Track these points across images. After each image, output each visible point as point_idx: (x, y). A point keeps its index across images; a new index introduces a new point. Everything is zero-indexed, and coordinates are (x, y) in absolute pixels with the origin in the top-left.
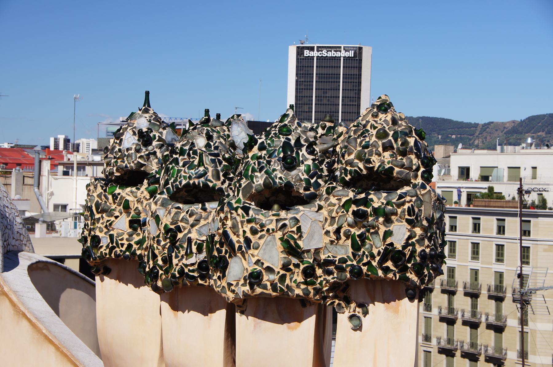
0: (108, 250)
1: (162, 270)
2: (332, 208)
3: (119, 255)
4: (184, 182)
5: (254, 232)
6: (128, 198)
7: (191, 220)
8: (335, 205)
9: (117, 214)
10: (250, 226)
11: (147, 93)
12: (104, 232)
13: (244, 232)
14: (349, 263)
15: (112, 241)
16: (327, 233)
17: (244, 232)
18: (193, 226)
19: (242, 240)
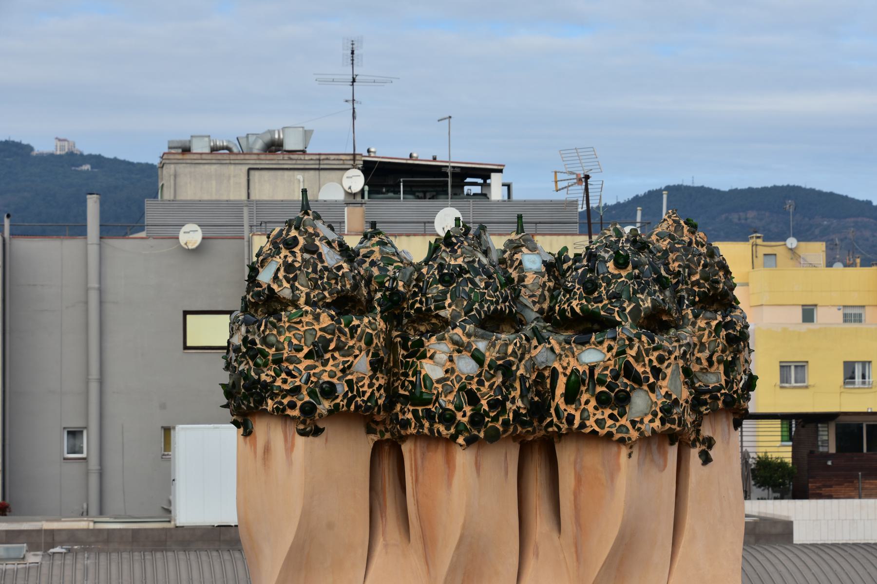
0: (345, 401)
1: (489, 417)
3: (361, 406)
4: (492, 308)
5: (661, 359)
6: (368, 330)
7: (519, 353)
8: (704, 329)
9: (357, 352)
10: (656, 354)
13: (651, 361)
14: (723, 391)
15: (351, 388)
16: (698, 359)
17: (651, 361)
18: (520, 361)
19: (648, 370)
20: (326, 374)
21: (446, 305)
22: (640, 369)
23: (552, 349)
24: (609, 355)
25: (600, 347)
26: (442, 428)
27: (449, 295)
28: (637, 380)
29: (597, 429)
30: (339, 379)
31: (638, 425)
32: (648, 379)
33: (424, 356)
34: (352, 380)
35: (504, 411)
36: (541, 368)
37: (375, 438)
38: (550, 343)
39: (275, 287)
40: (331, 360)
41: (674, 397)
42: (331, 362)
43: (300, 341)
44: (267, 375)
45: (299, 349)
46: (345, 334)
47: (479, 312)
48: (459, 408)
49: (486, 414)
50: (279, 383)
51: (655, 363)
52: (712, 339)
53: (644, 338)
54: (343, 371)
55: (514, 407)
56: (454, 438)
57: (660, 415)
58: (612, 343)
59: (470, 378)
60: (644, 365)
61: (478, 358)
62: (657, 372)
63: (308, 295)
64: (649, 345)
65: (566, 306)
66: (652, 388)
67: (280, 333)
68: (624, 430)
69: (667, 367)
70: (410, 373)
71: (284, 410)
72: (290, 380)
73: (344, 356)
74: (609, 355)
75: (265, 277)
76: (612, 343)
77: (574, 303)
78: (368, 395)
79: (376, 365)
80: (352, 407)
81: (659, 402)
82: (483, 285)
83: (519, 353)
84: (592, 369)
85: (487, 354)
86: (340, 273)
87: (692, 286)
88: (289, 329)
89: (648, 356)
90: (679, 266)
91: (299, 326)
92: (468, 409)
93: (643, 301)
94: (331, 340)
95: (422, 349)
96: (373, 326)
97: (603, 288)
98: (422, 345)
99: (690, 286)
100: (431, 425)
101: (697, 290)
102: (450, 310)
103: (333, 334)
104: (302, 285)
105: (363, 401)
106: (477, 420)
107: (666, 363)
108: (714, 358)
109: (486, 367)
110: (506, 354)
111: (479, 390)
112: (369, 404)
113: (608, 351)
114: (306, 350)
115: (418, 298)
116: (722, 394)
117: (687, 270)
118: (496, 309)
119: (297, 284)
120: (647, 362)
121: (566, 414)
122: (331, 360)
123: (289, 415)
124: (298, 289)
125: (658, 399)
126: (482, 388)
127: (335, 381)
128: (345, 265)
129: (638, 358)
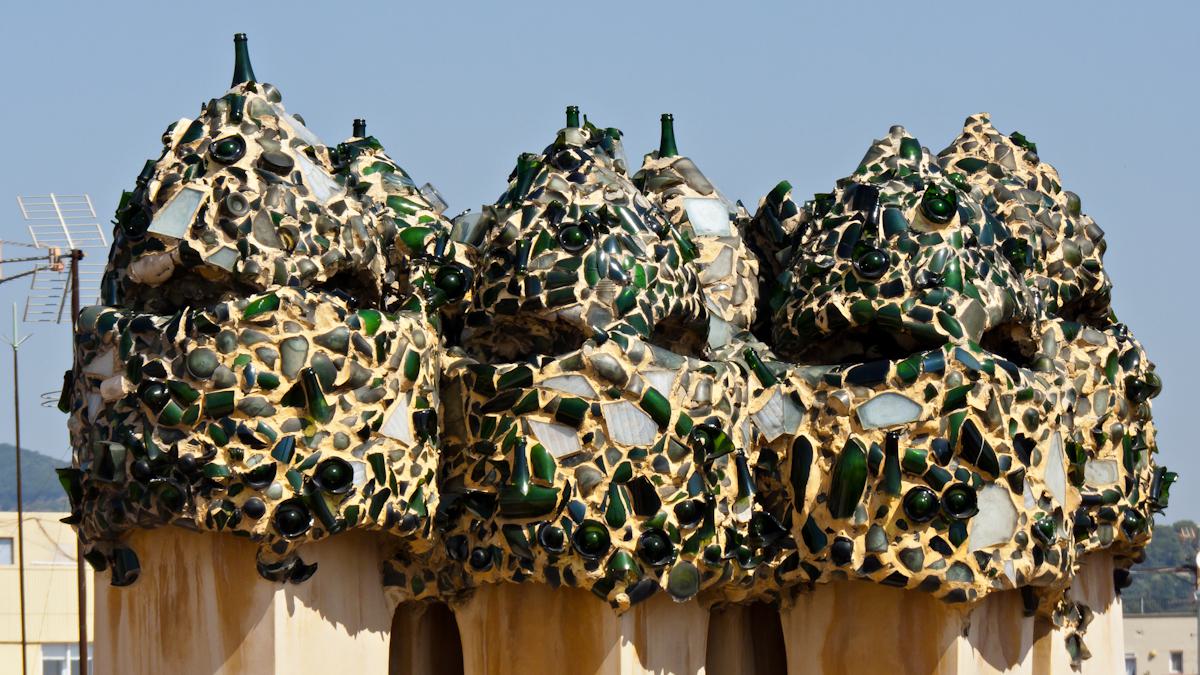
0: (369, 502)
2: (1080, 372)
4: (672, 302)
5: (1032, 421)
7: (732, 401)
9: (390, 395)
11: (240, 42)
12: (350, 449)
13: (1013, 423)
15: (380, 473)
17: (1013, 423)
19: (1009, 443)
20: (328, 440)
21: (577, 293)
22: (990, 439)
23: (795, 397)
24: (928, 408)
25: (908, 392)
26: (577, 566)
27: (581, 271)
28: (988, 466)
29: (904, 572)
30: (355, 452)
31: (992, 564)
32: (1008, 463)
33: (532, 405)
34: (380, 456)
35: (710, 528)
36: (770, 439)
37: (397, 594)
38: (788, 383)
39: (197, 245)
40: (339, 410)
41: (1055, 504)
42: (339, 414)
43: (271, 366)
44: (194, 442)
45: (268, 384)
46: (367, 353)
47: (647, 309)
48: (617, 521)
49: (677, 534)
50: (220, 460)
51: (1021, 429)
52: (1100, 386)
53: (1000, 373)
54: (364, 434)
55: (728, 523)
56: (604, 587)
57: (1031, 544)
58: (936, 383)
59: (636, 454)
60: (1000, 434)
61: (655, 409)
62: (1025, 447)
63: (279, 264)
64: (1010, 387)
65: (814, 305)
66: (1017, 483)
67: (222, 347)
68: (962, 573)
69: (1044, 437)
70: (499, 445)
71: (236, 520)
72: (248, 452)
73: (365, 401)
74: (928, 408)
75: (170, 223)
76: (936, 383)
77: (837, 299)
78: (410, 490)
79: (424, 425)
80: (382, 517)
81: (1031, 515)
82: (650, 251)
83: (732, 401)
84: (891, 443)
85: (673, 402)
86: (343, 219)
87: (1050, 275)
88: (245, 340)
89: (1007, 411)
90: (1023, 230)
91: (268, 333)
92: (633, 522)
93: (985, 294)
94: (338, 366)
95: (526, 392)
96: (419, 338)
97: (901, 266)
98: (529, 382)
99: (1045, 275)
100: (553, 558)
101: (1060, 282)
102: (587, 304)
103: (344, 351)
104: (265, 243)
105: (403, 503)
106: (656, 549)
107: (1041, 429)
108: (1107, 429)
109: (671, 431)
110: (708, 402)
111: (659, 481)
112: (412, 512)
113: (927, 400)
114: (285, 386)
115: (506, 280)
116: (1121, 509)
117: (1038, 239)
118: (678, 305)
119: (251, 239)
120: (1006, 425)
121: (831, 539)
122: (339, 410)
123: (245, 534)
124: (255, 250)
125: (1028, 505)
126: (664, 478)
127: (346, 456)
128: (350, 202)
129: (987, 417)
